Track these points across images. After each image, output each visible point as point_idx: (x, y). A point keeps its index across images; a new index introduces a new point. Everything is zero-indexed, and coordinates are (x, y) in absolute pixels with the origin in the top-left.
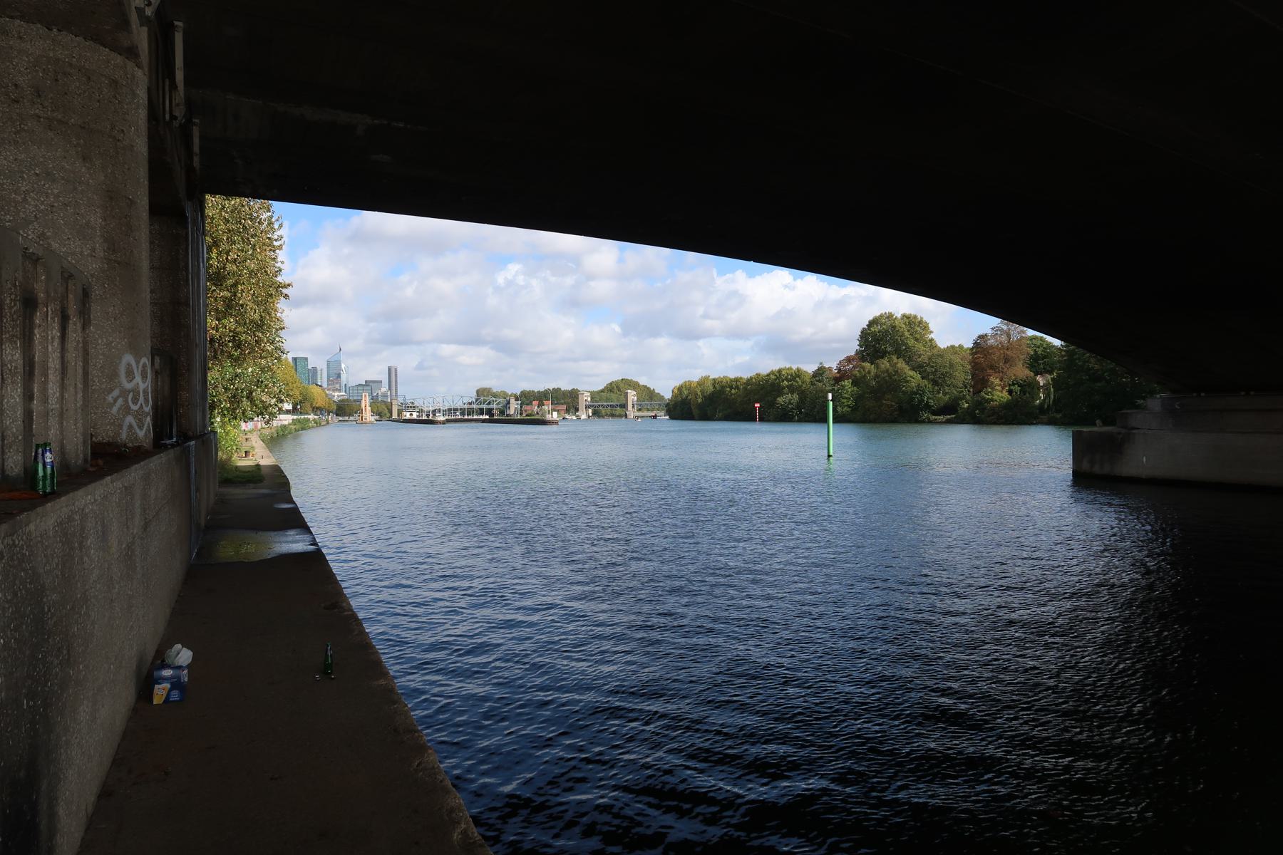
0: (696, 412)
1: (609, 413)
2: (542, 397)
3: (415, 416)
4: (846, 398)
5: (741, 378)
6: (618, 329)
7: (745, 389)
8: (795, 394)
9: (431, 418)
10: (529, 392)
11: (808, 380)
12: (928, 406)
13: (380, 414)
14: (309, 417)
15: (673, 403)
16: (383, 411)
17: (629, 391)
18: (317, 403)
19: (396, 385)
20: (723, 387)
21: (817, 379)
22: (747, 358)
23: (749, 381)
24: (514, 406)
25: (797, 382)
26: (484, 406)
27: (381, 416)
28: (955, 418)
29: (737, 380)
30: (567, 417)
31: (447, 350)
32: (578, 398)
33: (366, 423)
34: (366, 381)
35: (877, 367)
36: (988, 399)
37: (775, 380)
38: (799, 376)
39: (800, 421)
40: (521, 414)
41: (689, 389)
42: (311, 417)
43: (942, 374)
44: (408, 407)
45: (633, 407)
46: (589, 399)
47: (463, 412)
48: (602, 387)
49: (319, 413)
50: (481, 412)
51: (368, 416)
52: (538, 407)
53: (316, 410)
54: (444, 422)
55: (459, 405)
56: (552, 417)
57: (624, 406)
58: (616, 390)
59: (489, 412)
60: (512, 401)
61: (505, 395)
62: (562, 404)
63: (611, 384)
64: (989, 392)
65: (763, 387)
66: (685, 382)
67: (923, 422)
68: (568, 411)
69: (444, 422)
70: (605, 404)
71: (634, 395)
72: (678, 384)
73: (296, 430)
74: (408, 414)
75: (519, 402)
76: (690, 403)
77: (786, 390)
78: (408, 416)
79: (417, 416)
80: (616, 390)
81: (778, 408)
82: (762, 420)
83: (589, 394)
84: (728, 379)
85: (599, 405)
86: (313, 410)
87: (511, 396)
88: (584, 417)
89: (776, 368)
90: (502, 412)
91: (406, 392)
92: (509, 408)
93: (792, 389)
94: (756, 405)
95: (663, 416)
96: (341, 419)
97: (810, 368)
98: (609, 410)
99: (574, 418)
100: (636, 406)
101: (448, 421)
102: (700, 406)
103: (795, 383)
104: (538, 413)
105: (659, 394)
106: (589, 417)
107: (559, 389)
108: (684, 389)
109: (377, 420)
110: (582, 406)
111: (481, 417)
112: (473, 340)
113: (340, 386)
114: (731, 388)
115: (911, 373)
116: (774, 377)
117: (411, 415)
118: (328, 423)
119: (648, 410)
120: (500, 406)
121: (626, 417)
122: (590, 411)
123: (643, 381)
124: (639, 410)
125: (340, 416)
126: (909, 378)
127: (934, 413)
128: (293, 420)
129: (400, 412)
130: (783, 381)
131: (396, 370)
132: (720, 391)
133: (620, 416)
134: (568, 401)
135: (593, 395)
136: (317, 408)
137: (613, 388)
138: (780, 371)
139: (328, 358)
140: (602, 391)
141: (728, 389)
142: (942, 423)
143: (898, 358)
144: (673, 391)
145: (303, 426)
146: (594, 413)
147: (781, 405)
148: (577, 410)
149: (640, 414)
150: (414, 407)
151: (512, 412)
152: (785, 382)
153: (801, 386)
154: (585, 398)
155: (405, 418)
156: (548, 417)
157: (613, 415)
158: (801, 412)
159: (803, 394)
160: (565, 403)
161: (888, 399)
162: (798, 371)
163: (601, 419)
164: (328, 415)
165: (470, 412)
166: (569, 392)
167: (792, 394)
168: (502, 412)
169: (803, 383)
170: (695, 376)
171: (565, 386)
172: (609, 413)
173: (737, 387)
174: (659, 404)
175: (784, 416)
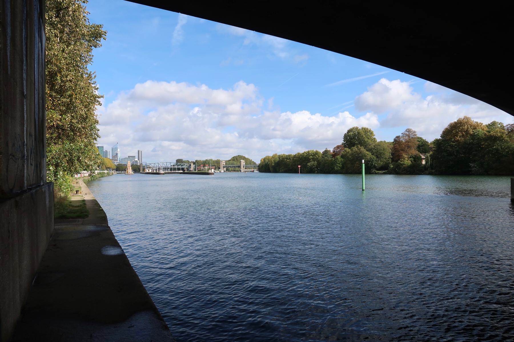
0: (271, 169)
1: (233, 170)
2: (205, 163)
3: (150, 171)
4: (338, 163)
5: (291, 155)
6: (237, 135)
7: (293, 159)
9: (157, 172)
11: (321, 156)
12: (375, 167)
14: (105, 171)
15: (261, 165)
16: (137, 169)
17: (242, 160)
18: (108, 166)
19: (141, 158)
20: (283, 159)
21: (325, 155)
22: (290, 147)
23: (295, 156)
24: (193, 166)
25: (316, 157)
26: (180, 167)
28: (387, 172)
29: (289, 156)
31: (166, 143)
32: (220, 164)
35: (352, 150)
36: (402, 164)
37: (307, 155)
38: (317, 154)
39: (318, 173)
41: (269, 160)
42: (106, 171)
43: (380, 153)
44: (147, 167)
45: (243, 167)
46: (225, 164)
47: (171, 169)
49: (109, 170)
50: (179, 169)
51: (130, 170)
52: (203, 167)
53: (107, 168)
54: (163, 174)
55: (169, 166)
56: (211, 171)
57: (239, 167)
60: (192, 164)
63: (234, 157)
64: (403, 161)
65: (301, 159)
67: (373, 173)
69: (163, 174)
70: (232, 166)
71: (244, 162)
72: (264, 157)
73: (99, 177)
74: (148, 170)
76: (269, 165)
77: (311, 160)
78: (147, 171)
79: (151, 171)
80: (236, 160)
82: (301, 173)
83: (224, 162)
84: (285, 156)
85: (229, 166)
86: (106, 168)
87: (191, 162)
88: (222, 171)
89: (307, 150)
91: (145, 161)
92: (191, 167)
93: (314, 160)
94: (299, 166)
95: (256, 171)
96: (118, 172)
97: (321, 151)
98: (233, 169)
100: (244, 167)
101: (165, 173)
102: (274, 167)
103: (315, 157)
104: (203, 170)
106: (225, 171)
107: (211, 160)
108: (266, 160)
110: (222, 167)
111: (179, 171)
112: (177, 140)
113: (117, 158)
114: (287, 159)
115: (367, 152)
116: (306, 154)
117: (149, 170)
118: (113, 174)
122: (225, 169)
123: (247, 156)
124: (246, 168)
125: (118, 171)
126: (366, 155)
127: (377, 170)
128: (98, 173)
130: (310, 156)
131: (141, 152)
132: (282, 160)
133: (238, 171)
134: (217, 165)
135: (226, 161)
136: (108, 168)
138: (308, 152)
139: (112, 147)
140: (230, 160)
141: (286, 160)
142: (381, 174)
143: (361, 146)
144: (261, 161)
145: (102, 175)
146: (227, 170)
148: (219, 168)
149: (246, 170)
150: (150, 167)
152: (311, 157)
153: (317, 158)
155: (146, 172)
156: (210, 171)
157: (234, 171)
158: (318, 169)
159: (318, 161)
160: (214, 165)
161: (357, 164)
162: (317, 152)
164: (113, 171)
165: (175, 169)
166: (216, 161)
169: (318, 157)
170: (271, 154)
171: (214, 158)
173: (289, 159)
174: (254, 166)
175: (311, 171)
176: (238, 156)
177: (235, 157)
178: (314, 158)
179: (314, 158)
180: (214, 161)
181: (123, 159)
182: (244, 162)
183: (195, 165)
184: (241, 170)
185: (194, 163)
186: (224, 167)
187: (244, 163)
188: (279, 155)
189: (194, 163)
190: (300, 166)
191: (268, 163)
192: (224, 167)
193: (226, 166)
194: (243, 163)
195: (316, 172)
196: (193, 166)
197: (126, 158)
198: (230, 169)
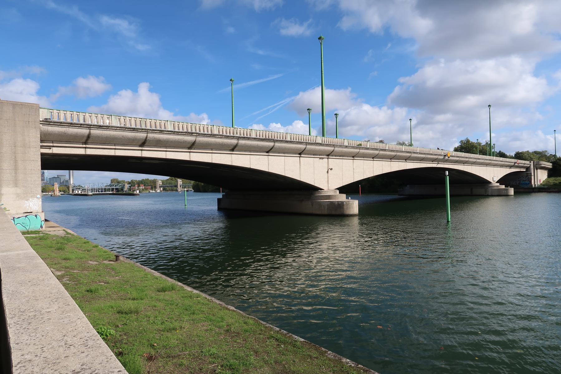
3: (80, 192)
13: (64, 191)
17: (178, 180)
24: (127, 186)
27: (65, 192)
33: (56, 196)
34: (58, 176)
40: (131, 190)
44: (77, 188)
45: (180, 187)
46: (161, 183)
51: (58, 193)
57: (176, 186)
59: (113, 190)
61: (124, 181)
62: (149, 186)
68: (152, 189)
71: (180, 182)
75: (130, 185)
78: (77, 192)
79: (81, 192)
88: (159, 191)
90: (122, 189)
96: (44, 194)
99: (154, 192)
106: (161, 191)
109: (61, 194)
110: (158, 186)
113: (44, 178)
117: (78, 192)
120: (120, 187)
122: (162, 188)
125: (44, 192)
129: (73, 190)
133: (175, 190)
146: (163, 190)
155: (75, 193)
157: (172, 190)
160: (150, 185)
165: (105, 190)
172: (170, 189)
181: (50, 178)
182: (180, 182)
183: (130, 185)
184: (178, 189)
186: (160, 187)
187: (181, 183)
189: (129, 183)
192: (160, 187)
194: (180, 183)
196: (127, 186)
197: (54, 177)
198: (168, 188)
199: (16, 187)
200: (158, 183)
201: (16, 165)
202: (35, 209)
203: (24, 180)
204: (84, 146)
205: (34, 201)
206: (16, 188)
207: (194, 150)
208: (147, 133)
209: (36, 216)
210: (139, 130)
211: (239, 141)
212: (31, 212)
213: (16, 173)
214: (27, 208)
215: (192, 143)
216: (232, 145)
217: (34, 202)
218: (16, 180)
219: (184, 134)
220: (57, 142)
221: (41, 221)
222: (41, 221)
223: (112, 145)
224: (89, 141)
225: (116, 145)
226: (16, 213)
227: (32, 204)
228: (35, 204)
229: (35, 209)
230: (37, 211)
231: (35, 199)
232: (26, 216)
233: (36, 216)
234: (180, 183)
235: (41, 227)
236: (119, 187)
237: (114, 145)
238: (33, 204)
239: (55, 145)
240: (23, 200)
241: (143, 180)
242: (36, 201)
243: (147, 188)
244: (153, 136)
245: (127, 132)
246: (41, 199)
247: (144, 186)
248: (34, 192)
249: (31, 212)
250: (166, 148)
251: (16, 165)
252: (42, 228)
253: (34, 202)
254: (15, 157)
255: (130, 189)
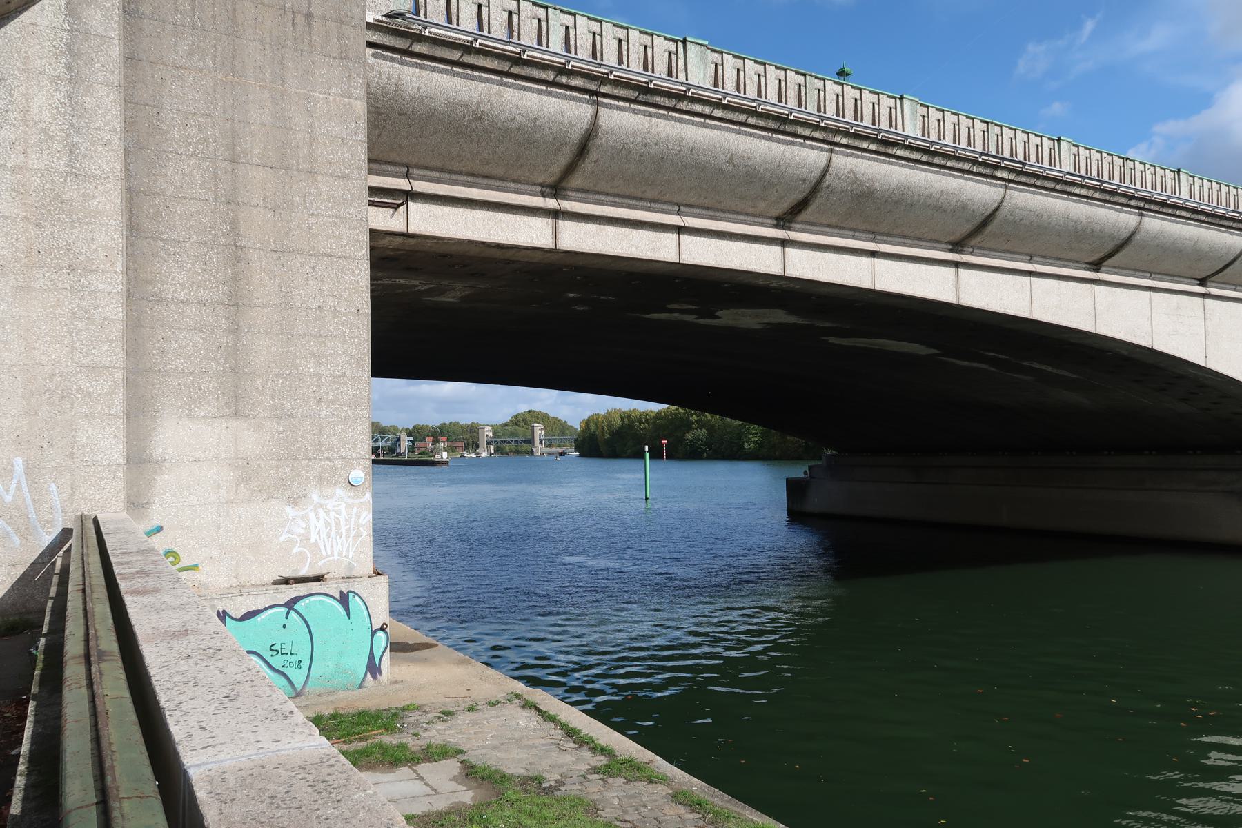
2: (437, 433)
5: (652, 412)
7: (654, 423)
8: (704, 430)
10: (422, 427)
15: (581, 438)
17: (536, 425)
20: (632, 422)
24: (405, 442)
25: (706, 417)
30: (466, 455)
32: (478, 433)
40: (413, 452)
41: (596, 423)
45: (541, 443)
46: (491, 434)
48: (506, 420)
57: (530, 442)
58: (522, 423)
62: (460, 440)
63: (516, 416)
66: (593, 416)
68: (466, 448)
70: (509, 439)
71: (541, 430)
75: (412, 439)
80: (522, 423)
81: (687, 444)
82: (670, 457)
84: (638, 414)
88: (484, 454)
90: (392, 450)
92: (400, 445)
94: (663, 442)
98: (513, 446)
99: (474, 456)
104: (432, 451)
105: (571, 426)
107: (456, 424)
108: (592, 424)
110: (482, 441)
119: (559, 446)
120: (388, 444)
121: (533, 455)
122: (492, 447)
124: (549, 446)
133: (527, 453)
137: (518, 421)
140: (506, 425)
141: (638, 424)
147: (690, 442)
148: (477, 446)
151: (402, 451)
153: (709, 421)
154: (487, 433)
157: (518, 452)
163: (504, 458)
167: (701, 429)
168: (392, 450)
171: (465, 419)
173: (647, 420)
176: (529, 411)
177: (519, 414)
178: (701, 420)
179: (701, 420)
180: (462, 428)
183: (412, 439)
184: (534, 449)
185: (410, 434)
186: (489, 443)
187: (543, 433)
188: (624, 413)
190: (666, 442)
191: (595, 432)
192: (489, 443)
193: (496, 441)
194: (540, 432)
195: (705, 455)
196: (405, 442)
198: (507, 447)
199: (237, 415)
200: (484, 434)
201: (235, 279)
202: (336, 557)
203: (278, 375)
204: (551, 203)
205: (330, 504)
206: (234, 424)
207: (971, 254)
208: (831, 151)
209: (344, 600)
210: (800, 131)
211: (1143, 218)
212: (319, 579)
213: (235, 329)
214: (294, 551)
215: (983, 217)
216: (1113, 239)
217: (333, 514)
218: (237, 371)
219: (967, 166)
220: (428, 173)
221: (373, 634)
222: (373, 634)
223: (670, 207)
224: (576, 181)
225: (683, 209)
226: (234, 582)
227: (321, 525)
228: (337, 523)
229: (336, 557)
230: (350, 567)
231: (340, 492)
232: (291, 604)
233: (344, 600)
234: (540, 432)
235: (373, 668)
236: (385, 444)
237: (676, 208)
238: (327, 524)
239: (420, 186)
240: (273, 502)
241: (445, 424)
242: (343, 505)
243: (456, 447)
244: (849, 167)
245: (751, 135)
246: (368, 496)
247: (448, 440)
248: (330, 448)
249: (319, 579)
250: (873, 240)
251: (235, 279)
252: (374, 677)
253: (333, 514)
254: (234, 223)
255: (412, 450)
